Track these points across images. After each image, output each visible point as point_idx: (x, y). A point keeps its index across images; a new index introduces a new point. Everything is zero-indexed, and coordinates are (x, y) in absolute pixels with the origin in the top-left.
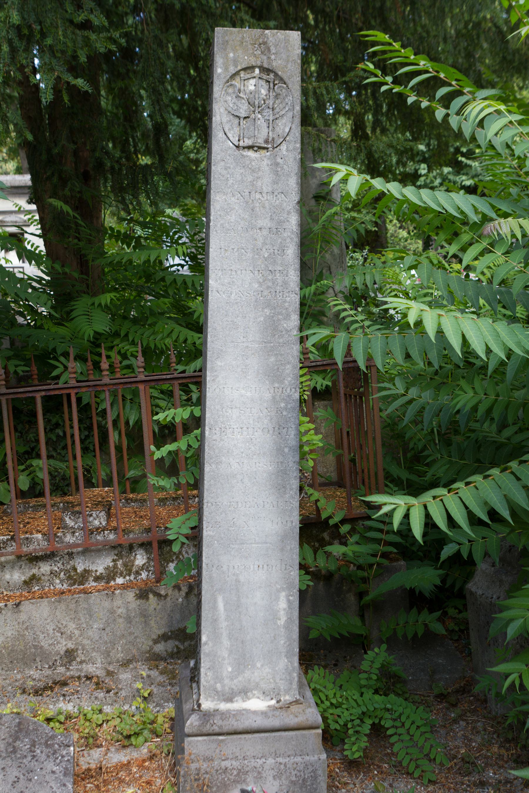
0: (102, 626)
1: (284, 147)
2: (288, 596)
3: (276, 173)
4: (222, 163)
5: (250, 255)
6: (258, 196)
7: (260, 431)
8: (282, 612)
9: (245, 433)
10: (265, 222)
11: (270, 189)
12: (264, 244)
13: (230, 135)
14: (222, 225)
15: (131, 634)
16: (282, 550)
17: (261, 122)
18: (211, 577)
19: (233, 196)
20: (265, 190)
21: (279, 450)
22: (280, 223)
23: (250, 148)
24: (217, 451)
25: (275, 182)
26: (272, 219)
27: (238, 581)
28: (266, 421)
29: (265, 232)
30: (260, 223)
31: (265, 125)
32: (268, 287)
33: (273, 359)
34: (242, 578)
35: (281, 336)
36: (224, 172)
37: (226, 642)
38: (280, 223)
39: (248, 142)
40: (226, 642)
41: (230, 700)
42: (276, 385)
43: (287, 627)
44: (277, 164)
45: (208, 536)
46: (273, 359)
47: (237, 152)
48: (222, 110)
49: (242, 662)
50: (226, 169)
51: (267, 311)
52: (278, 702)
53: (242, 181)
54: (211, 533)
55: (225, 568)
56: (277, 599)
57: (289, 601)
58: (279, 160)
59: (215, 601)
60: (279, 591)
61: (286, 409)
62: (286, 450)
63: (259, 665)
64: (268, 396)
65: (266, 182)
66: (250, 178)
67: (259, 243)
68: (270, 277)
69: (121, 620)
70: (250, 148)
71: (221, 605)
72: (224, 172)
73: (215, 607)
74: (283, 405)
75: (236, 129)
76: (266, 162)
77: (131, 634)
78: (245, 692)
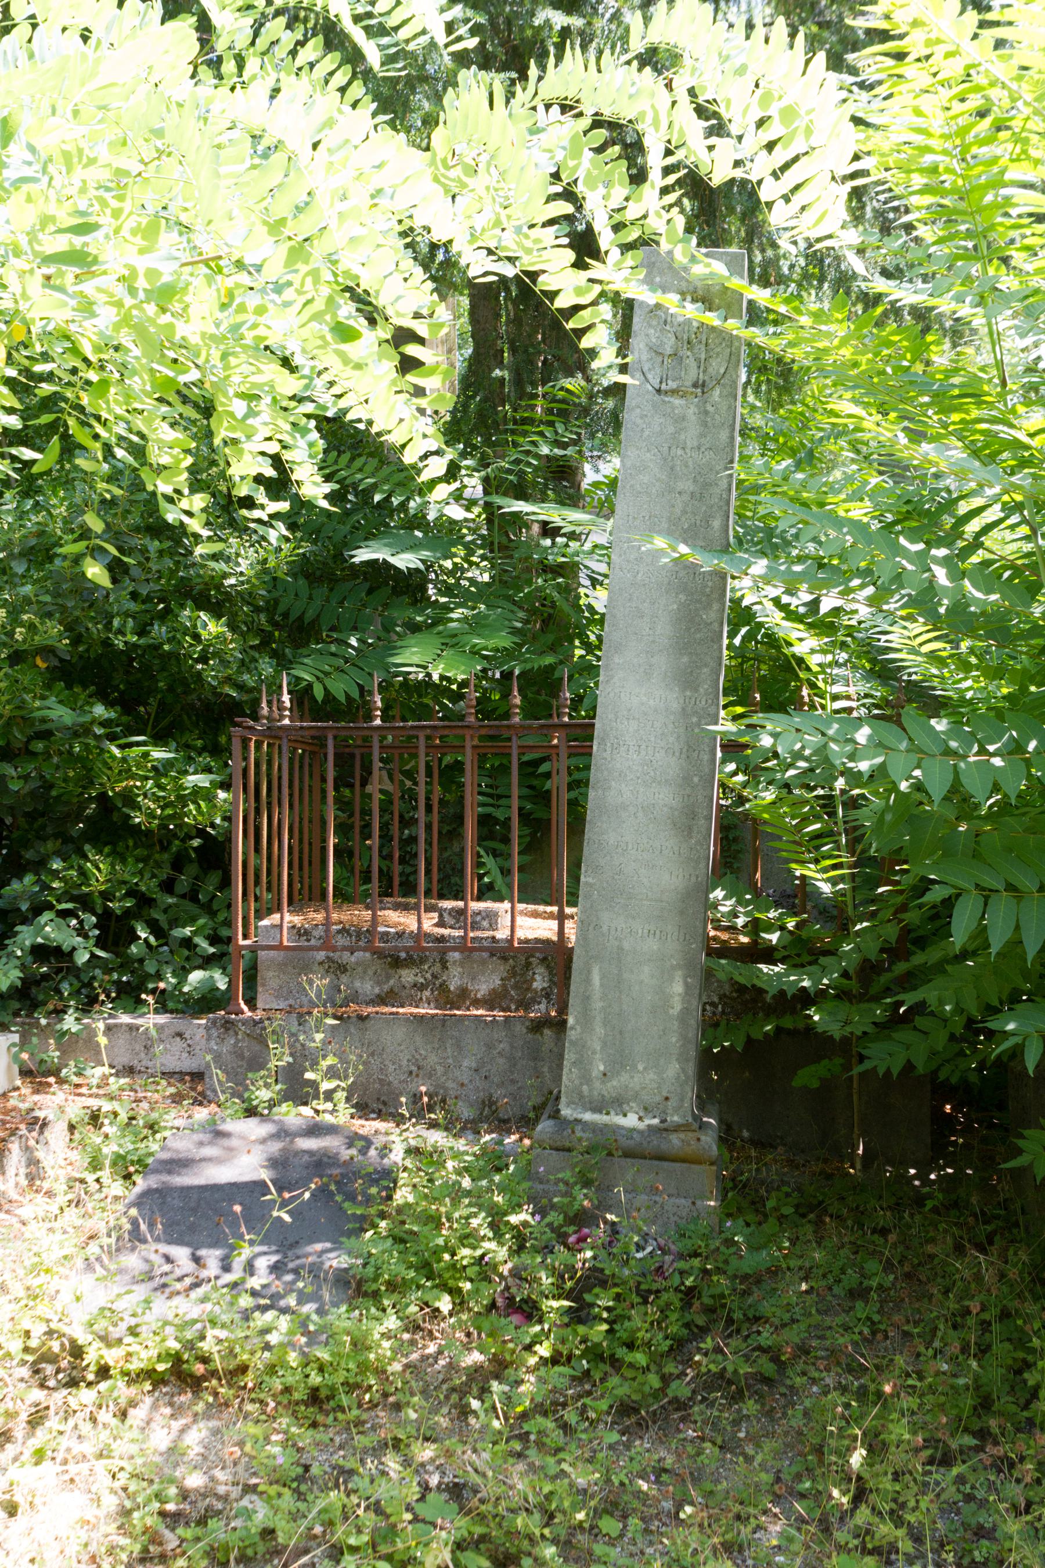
0: (474, 1065)
1: (717, 392)
2: (685, 977)
3: (705, 424)
6: (680, 452)
8: (677, 998)
10: (688, 485)
12: (684, 512)
13: (650, 376)
15: (513, 1082)
16: (682, 913)
17: (691, 363)
20: (689, 444)
21: (687, 779)
22: (706, 485)
23: (674, 392)
25: (702, 435)
26: (695, 481)
27: (620, 948)
28: (671, 739)
29: (686, 497)
30: (680, 485)
31: (693, 364)
33: (685, 659)
34: (626, 945)
35: (699, 630)
36: (639, 421)
37: (599, 1030)
38: (706, 485)
39: (672, 385)
40: (599, 1030)
43: (683, 1018)
44: (706, 412)
46: (685, 659)
47: (657, 397)
48: (642, 346)
49: (619, 1062)
51: (682, 597)
52: (663, 1121)
53: (661, 433)
54: (590, 880)
55: (605, 928)
56: (671, 979)
57: (686, 984)
58: (709, 408)
59: (589, 972)
60: (673, 968)
62: (696, 779)
63: (640, 1067)
64: (675, 706)
65: (691, 435)
66: (671, 429)
67: (678, 511)
69: (501, 1061)
70: (674, 392)
72: (639, 421)
73: (588, 981)
74: (695, 720)
75: (658, 370)
76: (692, 410)
77: (513, 1082)
78: (618, 1104)
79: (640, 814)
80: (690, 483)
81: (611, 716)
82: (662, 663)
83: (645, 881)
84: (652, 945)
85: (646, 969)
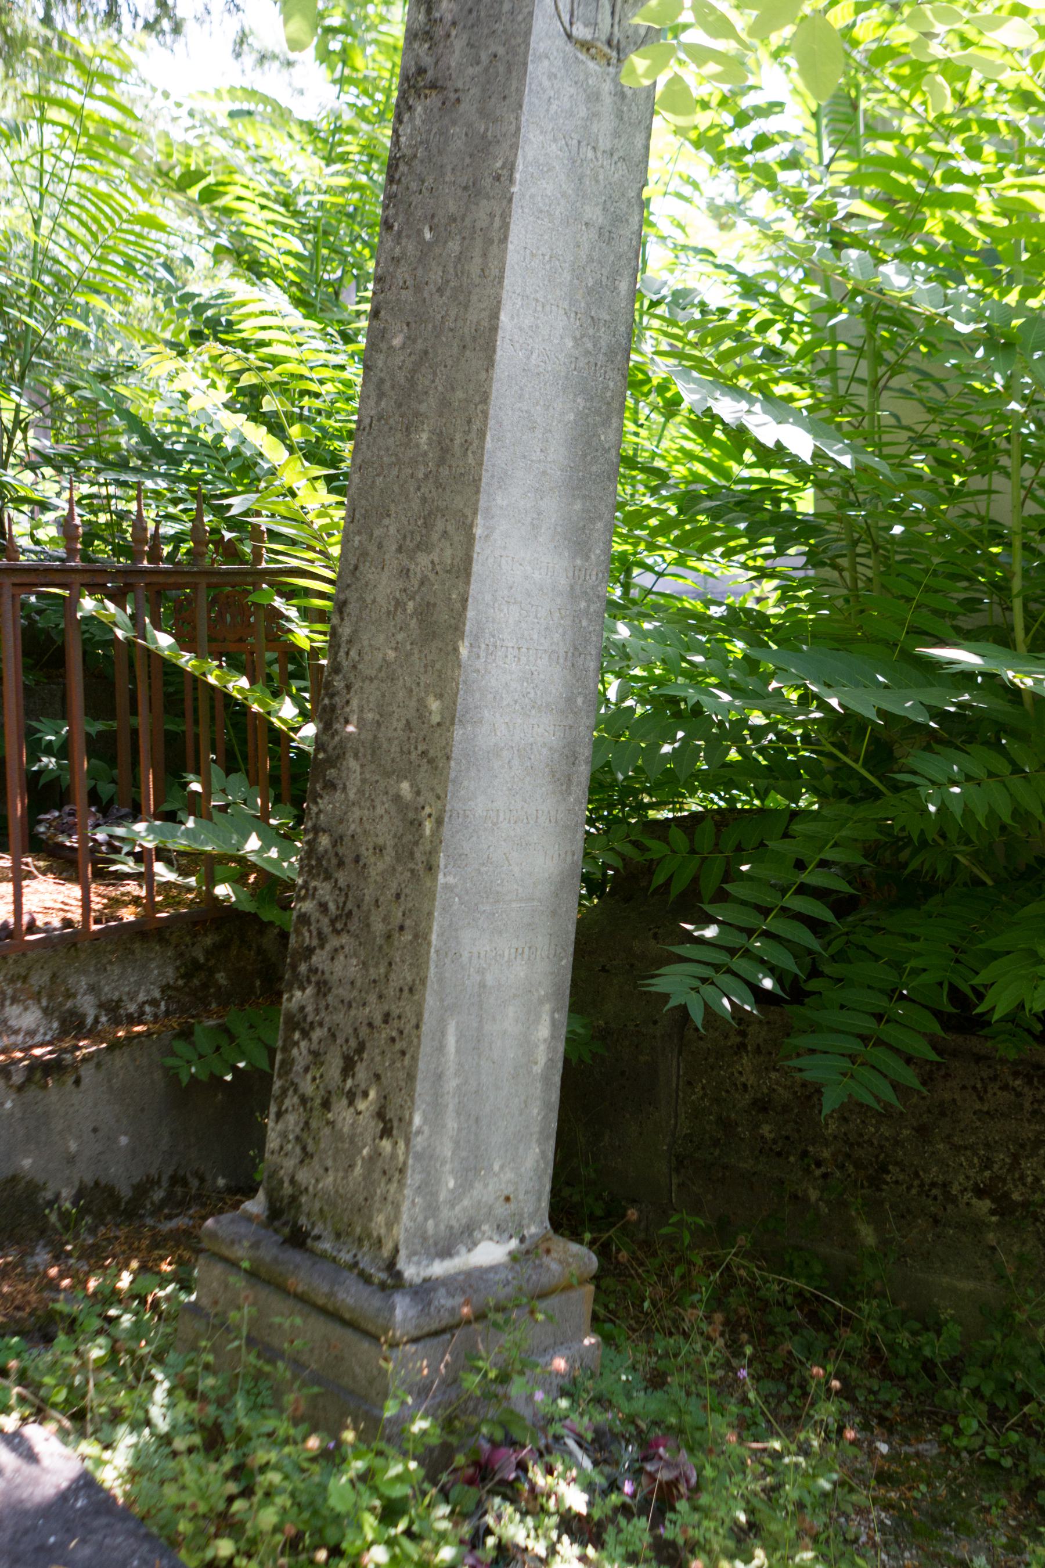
4: (546, 63)
5: (567, 276)
6: (590, 154)
7: (546, 657)
8: (542, 1047)
9: (524, 659)
10: (594, 213)
11: (609, 146)
12: (590, 259)
14: (532, 196)
18: (441, 980)
19: (555, 140)
20: (601, 146)
24: (477, 695)
27: (482, 985)
28: (557, 637)
29: (593, 234)
32: (588, 352)
36: (546, 83)
40: (451, 1124)
41: (446, 1252)
42: (579, 562)
43: (546, 1079)
45: (447, 887)
46: (578, 506)
50: (549, 78)
52: (522, 1240)
54: (451, 880)
55: (466, 955)
57: (553, 1021)
61: (587, 612)
62: (580, 701)
63: (496, 1167)
64: (563, 582)
67: (583, 254)
68: (591, 332)
71: (451, 1041)
73: (441, 1048)
74: (583, 605)
78: (467, 1234)
79: (516, 762)
80: (598, 210)
81: (488, 597)
82: (552, 507)
83: (516, 870)
84: (519, 971)
85: (511, 1011)
